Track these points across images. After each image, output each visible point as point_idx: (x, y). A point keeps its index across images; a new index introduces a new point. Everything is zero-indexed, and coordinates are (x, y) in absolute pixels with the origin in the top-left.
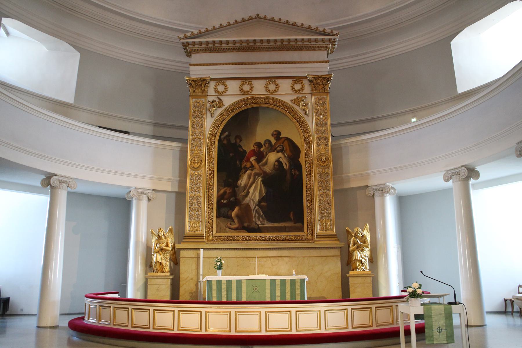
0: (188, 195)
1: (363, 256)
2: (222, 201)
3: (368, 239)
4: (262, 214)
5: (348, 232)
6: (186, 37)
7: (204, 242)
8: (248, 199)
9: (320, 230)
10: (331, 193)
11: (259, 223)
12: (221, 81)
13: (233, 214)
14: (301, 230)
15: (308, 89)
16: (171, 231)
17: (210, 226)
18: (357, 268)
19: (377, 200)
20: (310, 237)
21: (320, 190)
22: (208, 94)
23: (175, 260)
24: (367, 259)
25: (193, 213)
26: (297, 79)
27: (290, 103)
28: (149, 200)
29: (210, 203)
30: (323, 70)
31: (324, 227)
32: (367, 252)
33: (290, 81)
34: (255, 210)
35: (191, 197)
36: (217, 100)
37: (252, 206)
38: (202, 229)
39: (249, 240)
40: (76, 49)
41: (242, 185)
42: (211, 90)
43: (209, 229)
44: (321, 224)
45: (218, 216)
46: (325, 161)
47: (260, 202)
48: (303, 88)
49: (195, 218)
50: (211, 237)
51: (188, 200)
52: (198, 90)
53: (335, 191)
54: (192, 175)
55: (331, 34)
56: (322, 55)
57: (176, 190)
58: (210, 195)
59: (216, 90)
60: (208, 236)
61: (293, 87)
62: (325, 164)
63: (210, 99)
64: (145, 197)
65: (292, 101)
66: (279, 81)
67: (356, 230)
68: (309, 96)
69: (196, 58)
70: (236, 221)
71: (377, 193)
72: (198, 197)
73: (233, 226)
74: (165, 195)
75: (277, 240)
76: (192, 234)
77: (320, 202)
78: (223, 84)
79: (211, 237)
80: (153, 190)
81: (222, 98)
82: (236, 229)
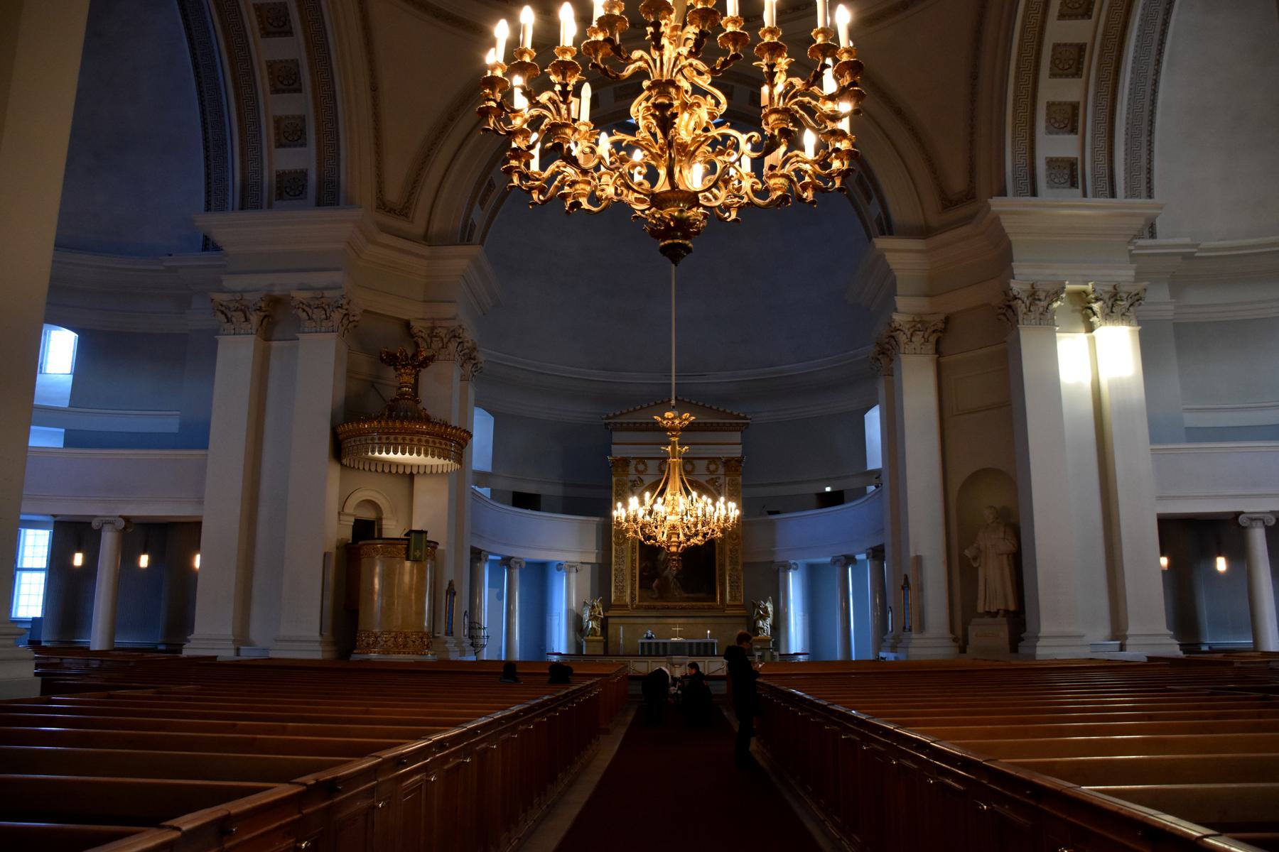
0: (613, 568)
1: (765, 624)
2: (644, 573)
3: (770, 609)
4: (678, 585)
5: (753, 604)
6: (608, 418)
7: (628, 610)
8: (667, 572)
9: (730, 600)
10: (740, 568)
11: (677, 594)
12: (641, 460)
13: (654, 585)
14: (714, 600)
15: (721, 470)
16: (600, 601)
17: (633, 596)
18: (759, 634)
19: (781, 574)
20: (721, 606)
21: (730, 565)
22: (630, 473)
23: (604, 624)
24: (769, 626)
25: (618, 584)
26: (713, 460)
27: (705, 483)
28: (577, 571)
29: (633, 576)
30: (736, 451)
31: (733, 598)
32: (769, 621)
33: (706, 462)
34: (673, 584)
35: (616, 570)
36: (637, 479)
37: (671, 577)
38: (628, 600)
39: (668, 608)
40: (490, 413)
41: (662, 559)
42: (632, 469)
43: (633, 599)
44: (731, 596)
45: (641, 587)
46: (735, 539)
47: (677, 574)
48: (717, 469)
49: (621, 590)
50: (634, 606)
51: (613, 572)
52: (620, 470)
53: (745, 565)
54: (616, 550)
55: (745, 418)
56: (737, 437)
57: (600, 561)
58: (633, 568)
59: (637, 470)
60: (632, 605)
61: (708, 469)
62: (736, 541)
63: (632, 478)
64: (574, 569)
65: (707, 481)
66: (695, 462)
67: (758, 603)
68: (722, 477)
69: (617, 436)
70: (656, 591)
71: (781, 568)
72: (622, 570)
73: (654, 596)
74: (589, 566)
75: (692, 608)
76: (617, 603)
77: (730, 576)
78: (644, 463)
79: (634, 606)
80: (582, 563)
81: (642, 477)
82: (656, 599)
